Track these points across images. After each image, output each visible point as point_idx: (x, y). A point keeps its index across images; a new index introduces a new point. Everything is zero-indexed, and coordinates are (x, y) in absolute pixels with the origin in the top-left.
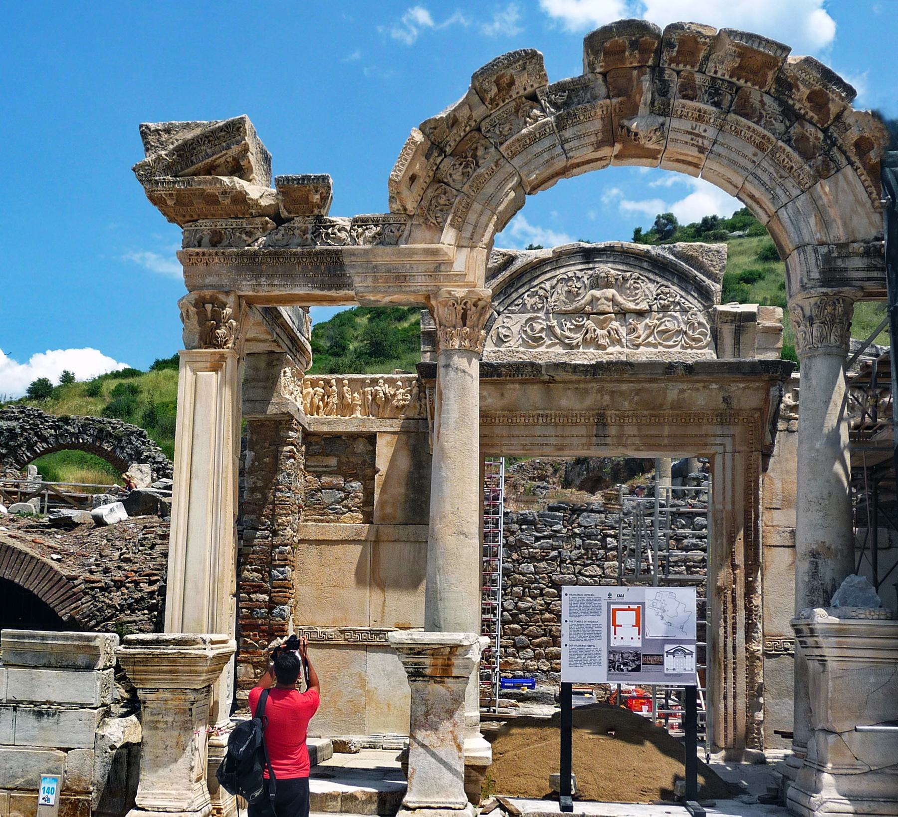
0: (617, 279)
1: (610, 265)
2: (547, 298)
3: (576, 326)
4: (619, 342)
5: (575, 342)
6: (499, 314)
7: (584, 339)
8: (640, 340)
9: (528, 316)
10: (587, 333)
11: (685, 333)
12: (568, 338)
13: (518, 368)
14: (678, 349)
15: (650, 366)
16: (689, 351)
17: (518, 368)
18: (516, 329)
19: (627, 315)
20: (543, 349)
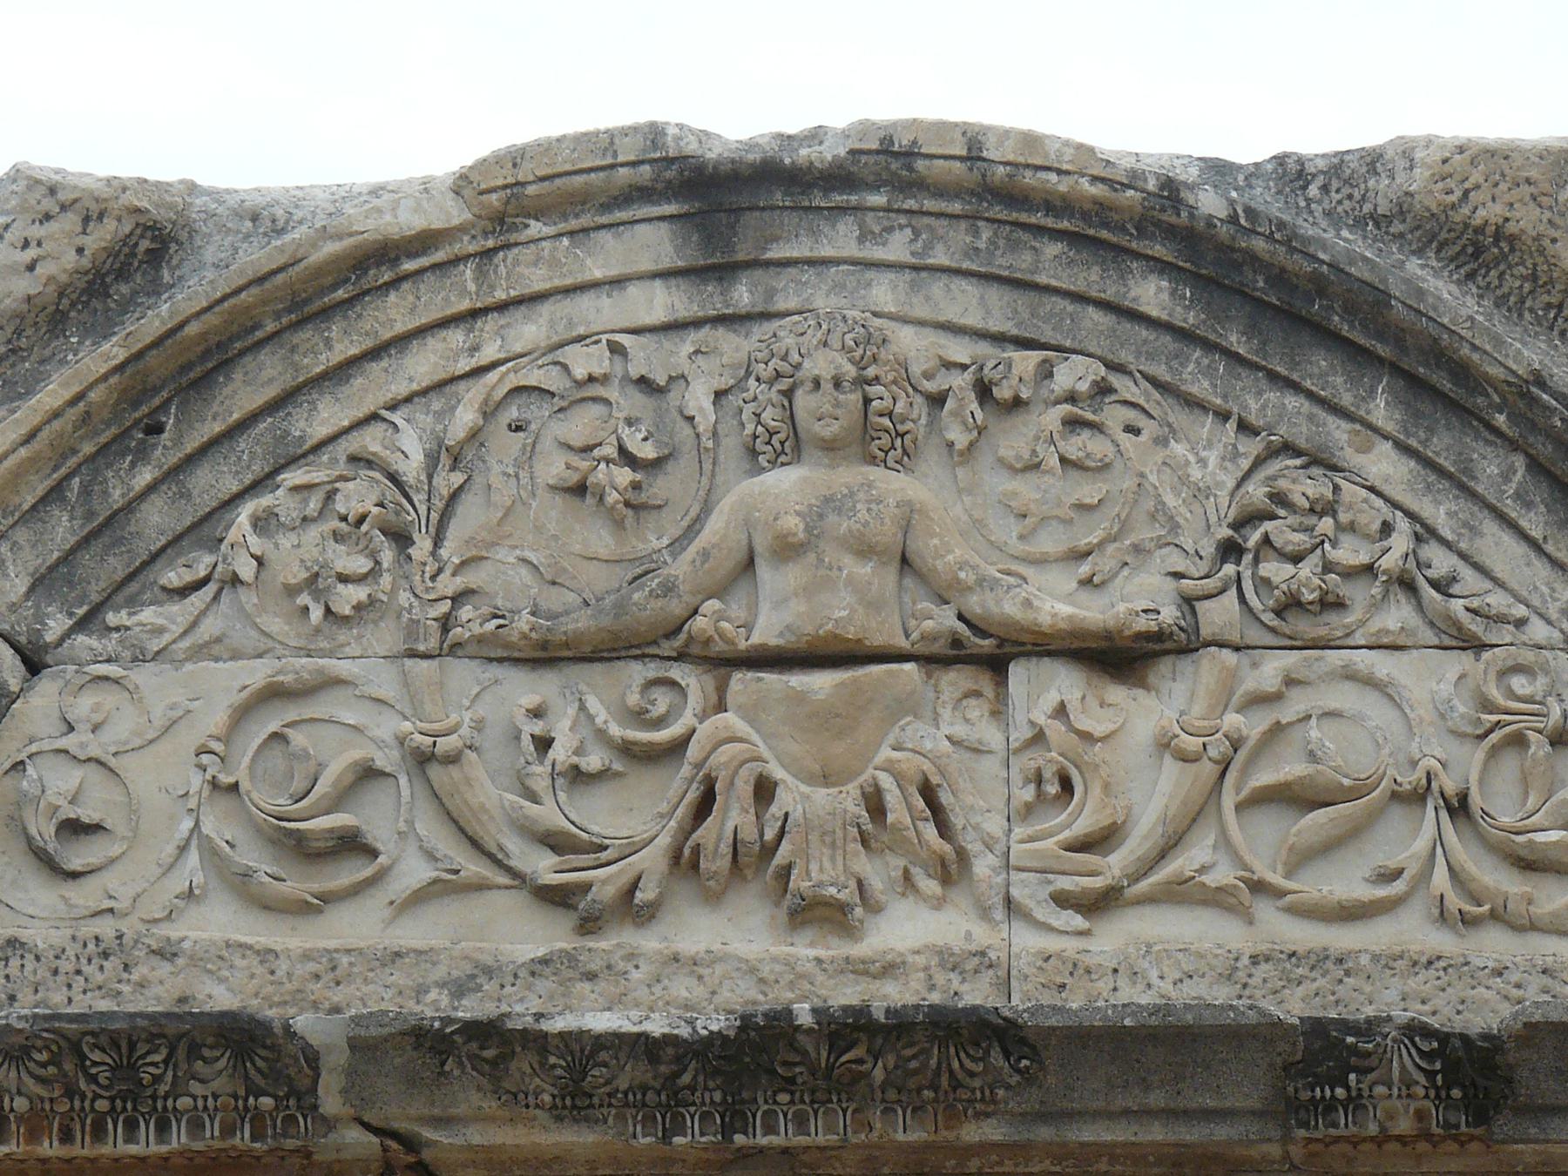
0: (937, 400)
1: (884, 293)
2: (401, 539)
3: (628, 750)
4: (952, 870)
5: (606, 881)
6: (33, 665)
7: (685, 862)
8: (1115, 864)
9: (257, 673)
10: (705, 806)
11: (1459, 808)
12: (556, 842)
13: (126, 1069)
14: (1409, 930)
15: (1163, 1048)
16: (1493, 944)
17: (126, 1069)
18: (163, 778)
19: (1018, 673)
20: (357, 926)
